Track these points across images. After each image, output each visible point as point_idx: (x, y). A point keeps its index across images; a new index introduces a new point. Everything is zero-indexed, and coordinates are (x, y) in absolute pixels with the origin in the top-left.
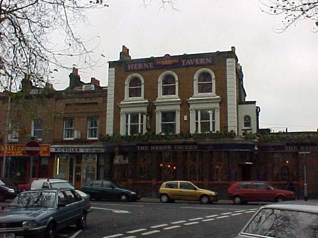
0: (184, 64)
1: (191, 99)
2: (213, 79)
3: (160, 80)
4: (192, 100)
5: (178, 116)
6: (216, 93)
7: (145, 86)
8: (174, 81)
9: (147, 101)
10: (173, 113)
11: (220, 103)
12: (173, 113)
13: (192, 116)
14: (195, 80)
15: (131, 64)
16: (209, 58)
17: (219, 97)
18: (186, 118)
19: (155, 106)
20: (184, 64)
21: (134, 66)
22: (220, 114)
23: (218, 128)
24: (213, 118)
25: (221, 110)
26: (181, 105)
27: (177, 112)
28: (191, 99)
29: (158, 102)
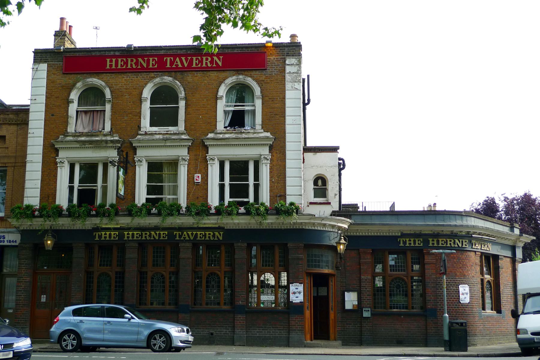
0: (168, 66)
1: (211, 135)
2: (258, 98)
3: (147, 93)
4: (213, 139)
5: (183, 171)
6: (262, 127)
7: (112, 107)
8: (175, 99)
9: (117, 138)
10: (174, 164)
11: (271, 148)
12: (174, 164)
13: (214, 171)
14: (221, 97)
15: (111, 57)
16: (143, 57)
17: (268, 134)
18: (198, 178)
19: (135, 149)
20: (168, 66)
21: (117, 62)
22: (271, 169)
23: (265, 197)
24: (222, 187)
25: (271, 160)
26: (189, 149)
27: (181, 162)
28: (211, 135)
29: (139, 141)
